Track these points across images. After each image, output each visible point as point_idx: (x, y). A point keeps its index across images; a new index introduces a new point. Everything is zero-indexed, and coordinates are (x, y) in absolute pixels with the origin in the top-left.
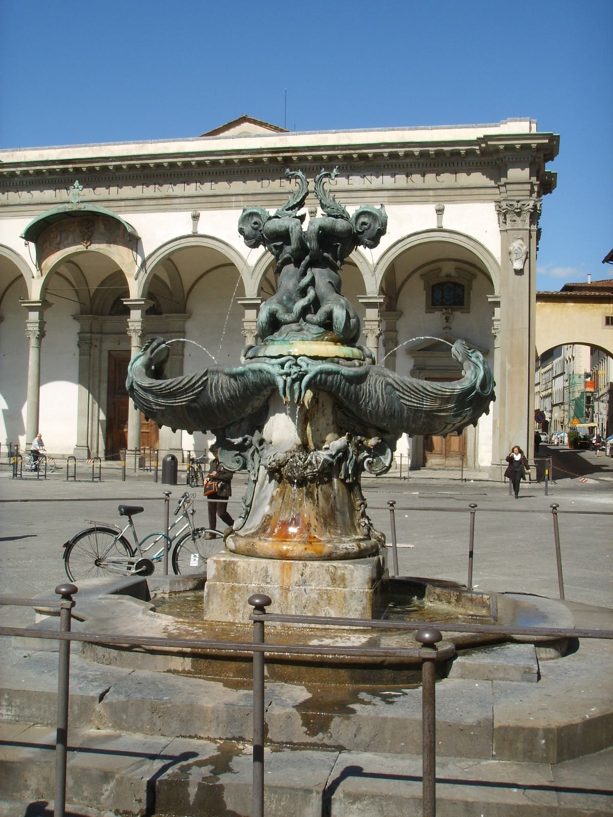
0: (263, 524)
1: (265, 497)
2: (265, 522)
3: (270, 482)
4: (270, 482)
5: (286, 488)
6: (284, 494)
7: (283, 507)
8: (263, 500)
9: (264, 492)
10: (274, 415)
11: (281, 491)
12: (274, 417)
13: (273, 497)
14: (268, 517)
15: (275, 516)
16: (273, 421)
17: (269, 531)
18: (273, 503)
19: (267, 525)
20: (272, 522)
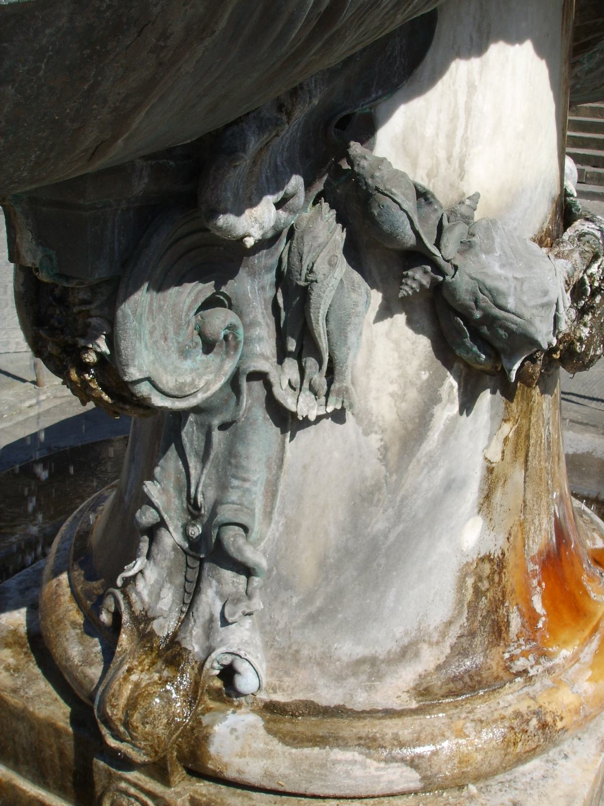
0: (473, 608)
1: (451, 486)
2: (478, 593)
3: (467, 404)
4: (467, 404)
5: (528, 412)
6: (528, 437)
7: (529, 496)
8: (437, 503)
9: (432, 462)
10: (478, 48)
11: (518, 433)
12: (475, 63)
13: (490, 470)
14: (487, 568)
15: (514, 548)
16: (472, 88)
17: (516, 622)
18: (498, 496)
19: (498, 604)
20: (511, 578)
